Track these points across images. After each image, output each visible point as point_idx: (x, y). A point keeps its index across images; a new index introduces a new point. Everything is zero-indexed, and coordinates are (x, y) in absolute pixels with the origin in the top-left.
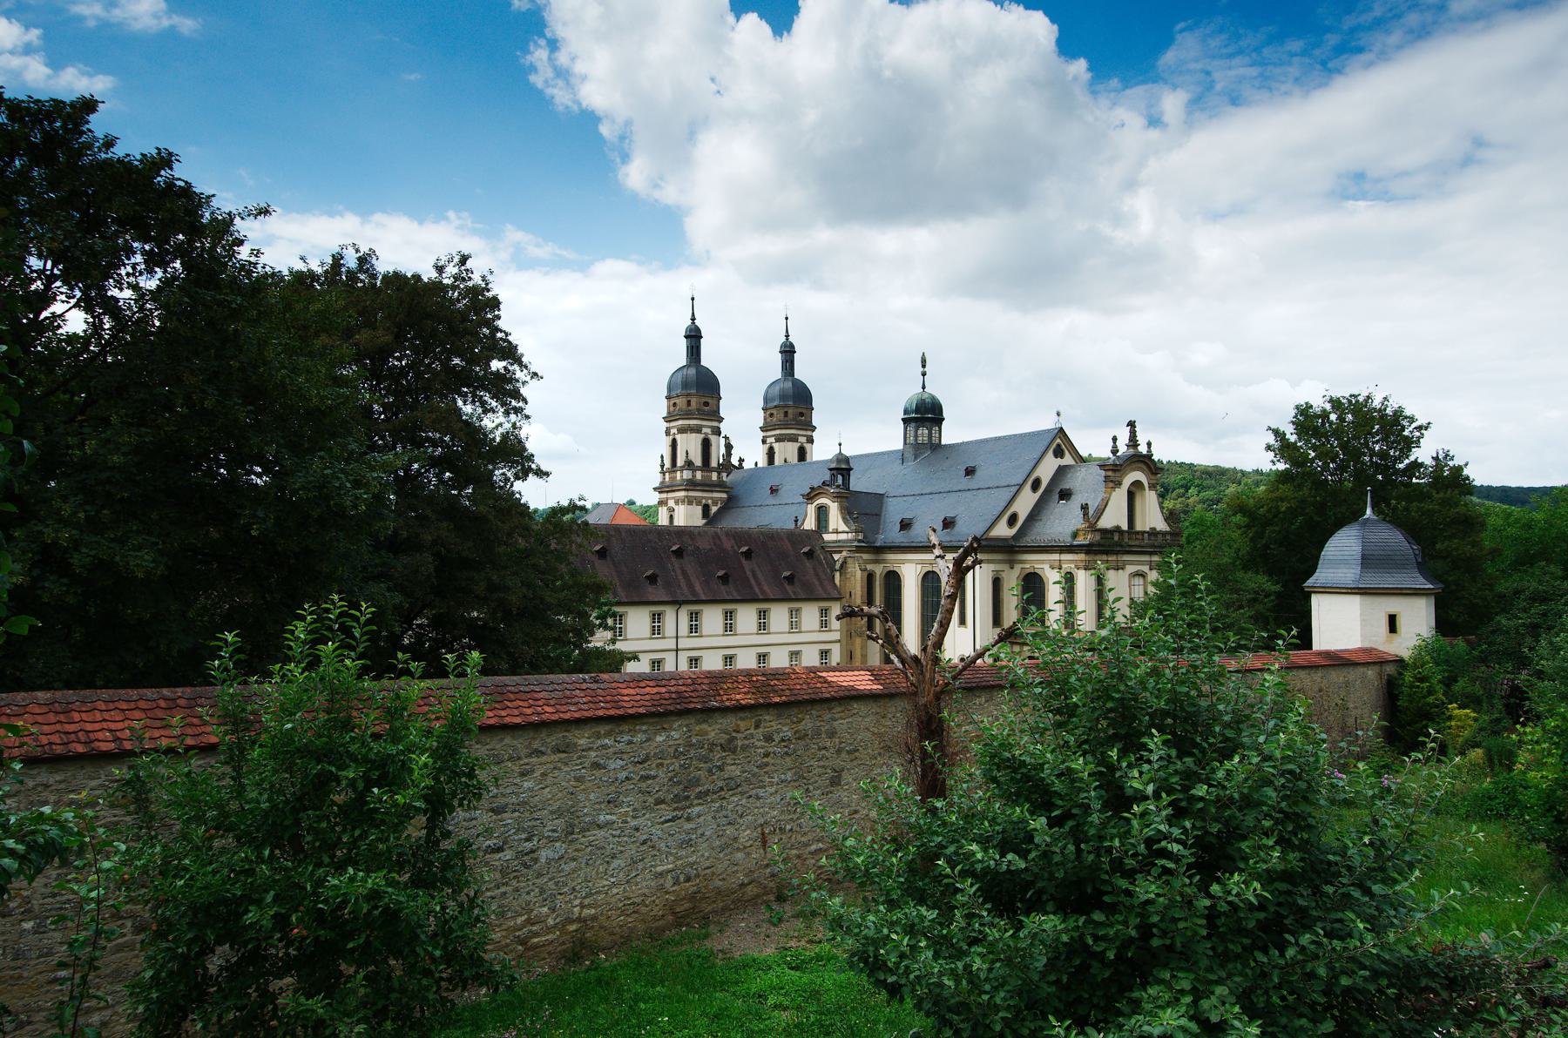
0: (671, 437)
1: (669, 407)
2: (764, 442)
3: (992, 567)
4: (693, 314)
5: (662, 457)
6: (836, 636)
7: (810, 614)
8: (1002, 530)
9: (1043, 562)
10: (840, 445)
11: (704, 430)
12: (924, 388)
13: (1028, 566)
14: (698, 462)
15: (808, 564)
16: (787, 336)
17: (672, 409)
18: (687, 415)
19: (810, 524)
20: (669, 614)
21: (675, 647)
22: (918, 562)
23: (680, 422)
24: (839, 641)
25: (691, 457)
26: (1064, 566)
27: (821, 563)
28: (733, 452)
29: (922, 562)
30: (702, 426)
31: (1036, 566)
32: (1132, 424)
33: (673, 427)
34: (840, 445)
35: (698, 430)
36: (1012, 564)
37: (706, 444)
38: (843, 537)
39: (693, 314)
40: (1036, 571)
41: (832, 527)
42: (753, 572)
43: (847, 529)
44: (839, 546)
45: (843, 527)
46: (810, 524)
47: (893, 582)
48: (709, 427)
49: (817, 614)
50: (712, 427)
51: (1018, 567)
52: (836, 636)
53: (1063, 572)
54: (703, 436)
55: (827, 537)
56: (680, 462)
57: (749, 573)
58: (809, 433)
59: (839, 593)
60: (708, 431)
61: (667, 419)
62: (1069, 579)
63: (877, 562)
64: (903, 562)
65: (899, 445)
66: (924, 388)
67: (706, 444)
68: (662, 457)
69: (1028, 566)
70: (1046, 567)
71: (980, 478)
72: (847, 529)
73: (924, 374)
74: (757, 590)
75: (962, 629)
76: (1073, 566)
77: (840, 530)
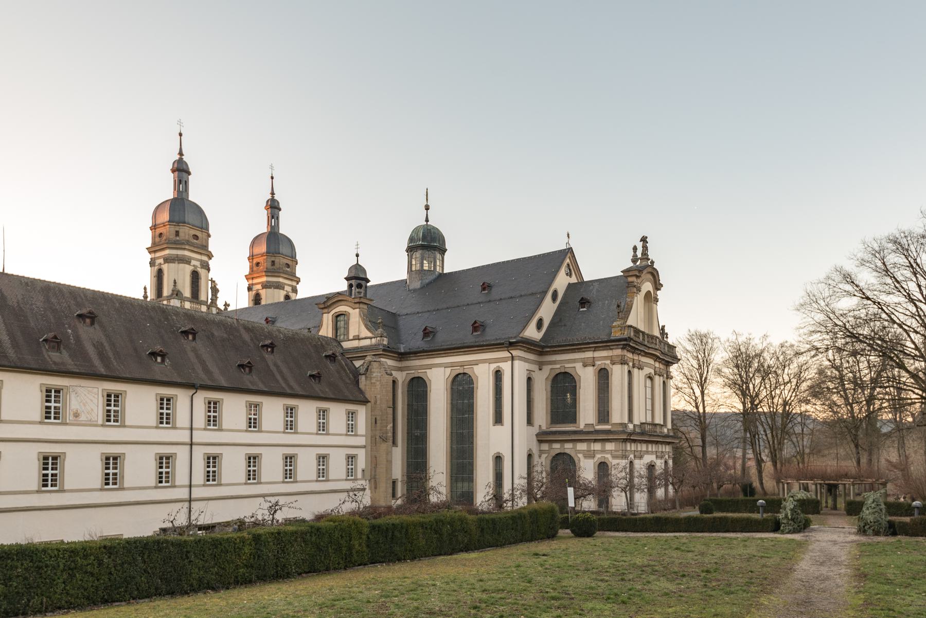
0: (156, 268)
1: (154, 238)
3: (527, 366)
5: (145, 288)
8: (532, 332)
9: (574, 361)
10: (357, 255)
11: (193, 262)
12: (427, 220)
13: (558, 366)
14: (187, 293)
15: (332, 366)
16: (273, 194)
17: (157, 239)
18: (176, 243)
19: (326, 331)
21: (188, 440)
23: (167, 252)
24: (364, 447)
25: (179, 287)
26: (598, 363)
28: (218, 295)
31: (567, 366)
32: (644, 240)
33: (159, 258)
34: (357, 255)
36: (541, 365)
37: (195, 276)
38: (366, 343)
40: (567, 370)
41: (352, 333)
43: (370, 335)
44: (360, 353)
45: (365, 333)
46: (326, 331)
49: (344, 417)
50: (201, 261)
51: (547, 369)
52: (361, 441)
53: (597, 368)
54: (192, 268)
55: (346, 345)
56: (166, 292)
57: (272, 368)
60: (198, 264)
61: (151, 250)
62: (603, 376)
63: (400, 369)
65: (403, 275)
66: (427, 220)
67: (195, 276)
68: (145, 288)
69: (558, 366)
70: (579, 366)
71: (496, 293)
72: (370, 335)
73: (427, 208)
74: (284, 385)
75: (498, 427)
76: (608, 362)
77: (362, 336)
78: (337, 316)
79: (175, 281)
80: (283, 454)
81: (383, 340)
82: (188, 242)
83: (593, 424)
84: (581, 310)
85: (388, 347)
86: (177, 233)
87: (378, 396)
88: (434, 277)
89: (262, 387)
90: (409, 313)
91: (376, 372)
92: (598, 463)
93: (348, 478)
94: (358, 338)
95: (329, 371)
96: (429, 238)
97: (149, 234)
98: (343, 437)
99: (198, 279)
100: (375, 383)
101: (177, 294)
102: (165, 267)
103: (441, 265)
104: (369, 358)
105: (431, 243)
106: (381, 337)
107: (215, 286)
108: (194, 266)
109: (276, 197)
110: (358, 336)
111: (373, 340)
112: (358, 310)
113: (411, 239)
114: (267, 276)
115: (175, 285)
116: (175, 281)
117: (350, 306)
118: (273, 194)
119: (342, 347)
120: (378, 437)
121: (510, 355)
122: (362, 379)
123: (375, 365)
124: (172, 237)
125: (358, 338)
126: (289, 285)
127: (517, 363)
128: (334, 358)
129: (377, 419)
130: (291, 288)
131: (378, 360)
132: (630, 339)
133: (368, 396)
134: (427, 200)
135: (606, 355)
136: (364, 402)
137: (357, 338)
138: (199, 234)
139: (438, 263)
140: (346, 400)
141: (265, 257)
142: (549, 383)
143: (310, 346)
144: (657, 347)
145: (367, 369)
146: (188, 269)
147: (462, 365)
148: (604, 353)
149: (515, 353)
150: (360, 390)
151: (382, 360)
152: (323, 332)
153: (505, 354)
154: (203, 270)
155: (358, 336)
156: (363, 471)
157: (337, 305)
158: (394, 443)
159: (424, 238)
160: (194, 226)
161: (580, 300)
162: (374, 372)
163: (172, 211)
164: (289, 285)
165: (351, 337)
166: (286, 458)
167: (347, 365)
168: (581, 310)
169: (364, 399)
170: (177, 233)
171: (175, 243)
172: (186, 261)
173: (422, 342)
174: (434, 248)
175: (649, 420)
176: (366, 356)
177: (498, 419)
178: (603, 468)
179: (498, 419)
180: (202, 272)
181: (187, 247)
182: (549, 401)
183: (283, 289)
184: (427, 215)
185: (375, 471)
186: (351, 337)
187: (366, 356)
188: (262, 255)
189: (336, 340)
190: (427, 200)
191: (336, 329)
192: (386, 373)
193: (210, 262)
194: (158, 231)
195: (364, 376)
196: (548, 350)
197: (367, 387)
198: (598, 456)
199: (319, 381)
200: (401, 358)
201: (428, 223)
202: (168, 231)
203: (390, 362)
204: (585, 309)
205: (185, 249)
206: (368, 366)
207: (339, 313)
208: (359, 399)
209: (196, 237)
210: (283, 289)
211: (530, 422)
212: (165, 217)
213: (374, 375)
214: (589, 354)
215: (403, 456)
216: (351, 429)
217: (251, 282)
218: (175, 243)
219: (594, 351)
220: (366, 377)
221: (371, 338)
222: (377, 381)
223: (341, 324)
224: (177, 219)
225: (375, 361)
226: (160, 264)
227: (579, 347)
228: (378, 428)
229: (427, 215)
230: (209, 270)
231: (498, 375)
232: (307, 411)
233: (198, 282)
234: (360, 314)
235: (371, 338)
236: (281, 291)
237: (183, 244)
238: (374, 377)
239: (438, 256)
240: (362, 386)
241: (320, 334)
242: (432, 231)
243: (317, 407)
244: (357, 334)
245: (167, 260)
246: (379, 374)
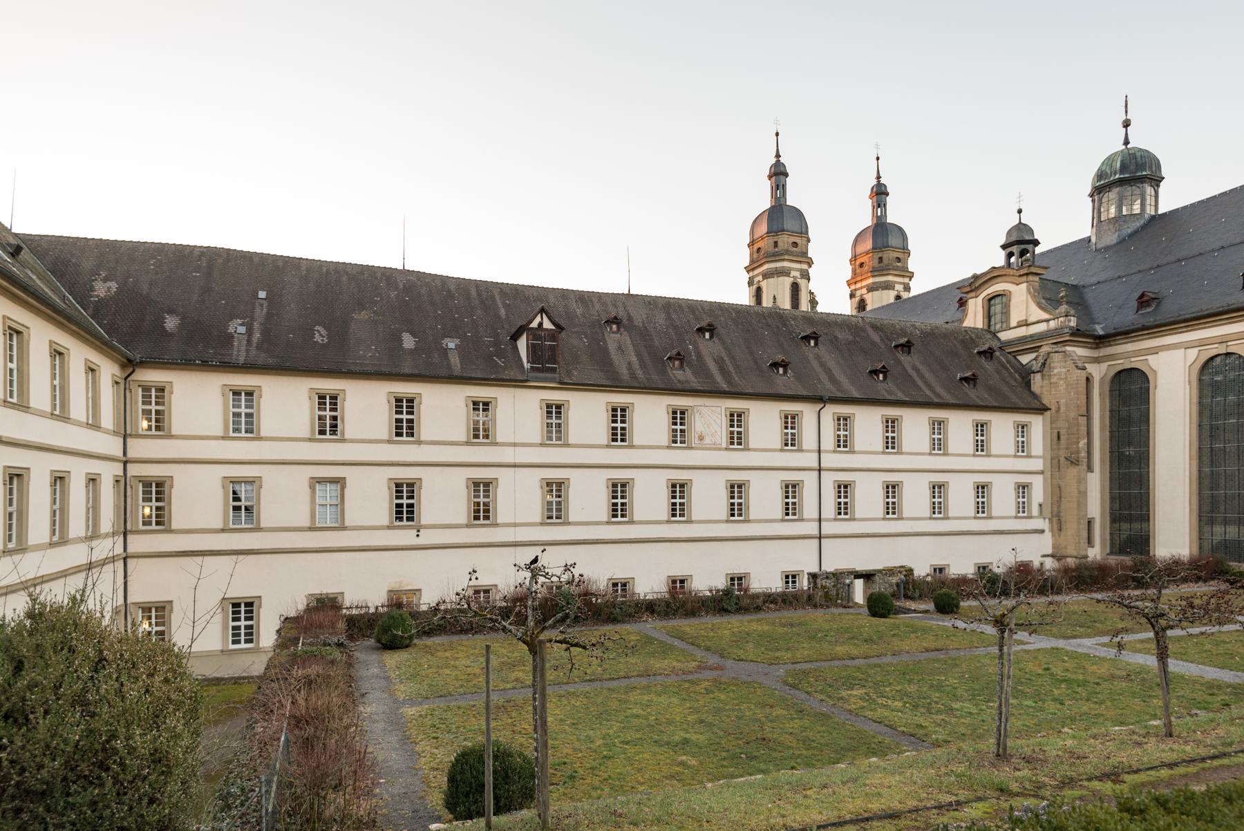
0: (755, 287)
1: (751, 255)
2: (852, 296)
4: (778, 150)
6: (1038, 465)
7: (1002, 426)
11: (793, 273)
12: (1126, 142)
15: (988, 365)
16: (879, 177)
17: (755, 256)
18: (775, 256)
19: (974, 317)
20: (807, 412)
21: (816, 465)
22: (1188, 346)
23: (766, 267)
29: (1201, 343)
30: (790, 269)
33: (757, 275)
37: (795, 288)
38: (1042, 327)
39: (778, 150)
42: (915, 368)
43: (1046, 316)
44: (1031, 343)
45: (1037, 314)
48: (797, 270)
55: (1005, 336)
57: (910, 371)
58: (906, 280)
60: (797, 274)
63: (1097, 360)
64: (1155, 351)
66: (1126, 142)
67: (795, 288)
72: (1045, 316)
74: (928, 393)
78: (990, 300)
79: (774, 297)
80: (930, 482)
81: (1070, 321)
82: (787, 252)
85: (1078, 330)
86: (776, 244)
87: (1062, 401)
88: (1142, 222)
89: (901, 396)
90: (1101, 280)
91: (1058, 367)
93: (1019, 515)
94: (1026, 324)
95: (985, 371)
96: (1132, 167)
97: (747, 251)
98: (1011, 459)
99: (798, 291)
100: (1056, 383)
102: (764, 284)
103: (1153, 203)
104: (1045, 349)
106: (1066, 316)
107: (814, 298)
109: (882, 181)
110: (1026, 320)
112: (1025, 285)
113: (1100, 175)
114: (873, 276)
116: (774, 297)
117: (1011, 282)
118: (879, 177)
120: (1062, 459)
122: (1037, 382)
123: (1056, 357)
124: (771, 249)
125: (1026, 324)
126: (900, 283)
128: (991, 354)
130: (902, 286)
131: (1060, 350)
133: (1046, 401)
134: (1126, 112)
136: (1041, 409)
137: (1024, 323)
138: (798, 240)
139: (1148, 202)
140: (1015, 408)
141: (871, 255)
143: (956, 342)
145: (1044, 364)
146: (787, 281)
147: (1223, 340)
150: (1034, 395)
151: (1068, 348)
152: (968, 323)
154: (803, 280)
155: (1026, 320)
156: (1040, 505)
157: (986, 286)
158: (1090, 469)
159: (1124, 167)
160: (793, 233)
162: (1054, 368)
163: (770, 220)
164: (900, 283)
165: (1013, 324)
166: (934, 487)
167: (1009, 362)
169: (1041, 406)
170: (776, 244)
171: (774, 255)
172: (784, 273)
173: (1136, 316)
174: (1142, 179)
176: (1041, 346)
180: (802, 282)
181: (786, 257)
183: (893, 288)
184: (1127, 134)
185: (1059, 506)
186: (1013, 324)
187: (1041, 346)
188: (867, 253)
189: (990, 331)
190: (1126, 112)
191: (989, 316)
192: (1077, 367)
193: (810, 271)
194: (756, 247)
195: (1039, 374)
197: (1044, 389)
199: (975, 386)
200: (1097, 344)
201: (1129, 146)
202: (766, 244)
203: (1080, 352)
205: (783, 260)
206: (1046, 360)
207: (991, 296)
208: (1033, 406)
209: (795, 244)
210: (893, 288)
212: (763, 228)
213: (1056, 371)
215: (1102, 486)
216: (1022, 448)
217: (853, 287)
218: (774, 255)
220: (1042, 376)
221: (1048, 321)
222: (1061, 379)
223: (997, 308)
224: (775, 228)
225: (1056, 352)
226: (759, 282)
229: (1127, 134)
230: (809, 280)
232: (960, 425)
233: (798, 294)
234: (1028, 290)
236: (891, 291)
237: (782, 254)
238: (1055, 375)
239: (1149, 190)
241: (965, 324)
242: (1138, 154)
243: (973, 420)
244: (1024, 318)
245: (766, 276)
246: (1064, 370)
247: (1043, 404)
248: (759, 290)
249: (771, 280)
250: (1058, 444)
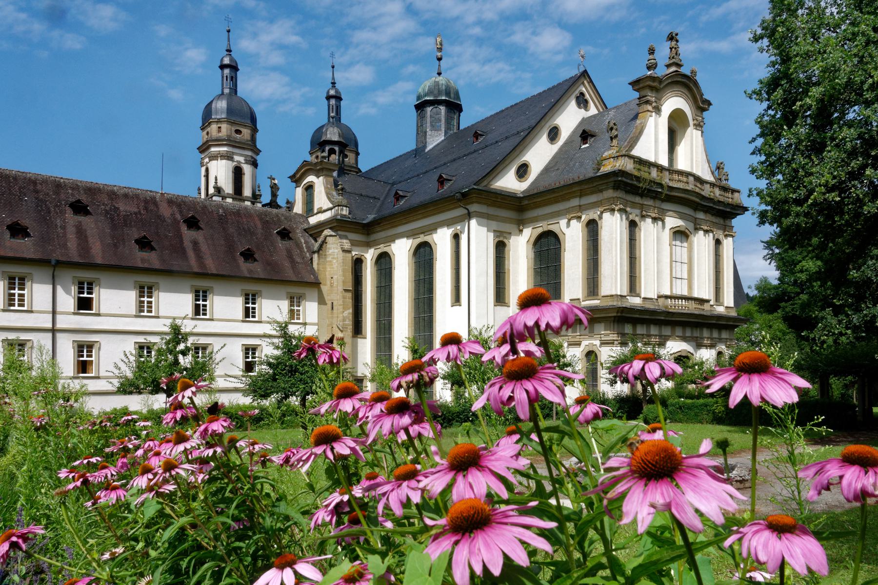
9: (558, 215)
14: (228, 188)
23: (213, 149)
27: (299, 246)
35: (229, 157)
36: (520, 224)
43: (331, 205)
47: (384, 262)
55: (313, 220)
59: (316, 278)
60: (242, 159)
67: (238, 173)
77: (325, 208)
81: (342, 210)
83: (579, 299)
84: (583, 147)
87: (335, 277)
92: (585, 353)
94: (321, 211)
100: (331, 261)
101: (218, 190)
105: (437, 97)
106: (339, 206)
108: (237, 161)
111: (333, 210)
115: (216, 183)
119: (308, 223)
121: (466, 211)
127: (473, 222)
129: (334, 304)
132: (622, 173)
135: (595, 200)
142: (531, 246)
144: (690, 187)
145: (321, 246)
148: (593, 199)
149: (474, 208)
150: (313, 272)
153: (460, 212)
161: (582, 134)
162: (329, 249)
165: (315, 211)
168: (583, 147)
175: (681, 289)
177: (457, 300)
178: (591, 355)
179: (457, 300)
182: (532, 272)
186: (315, 211)
196: (526, 202)
198: (585, 343)
204: (587, 145)
211: (500, 298)
213: (331, 251)
214: (575, 202)
219: (581, 196)
221: (331, 209)
222: (333, 258)
226: (207, 163)
227: (561, 193)
228: (335, 315)
231: (456, 237)
235: (331, 209)
238: (330, 255)
240: (315, 266)
247: (318, 280)
248: (207, 170)
249: (214, 163)
250: (332, 313)
